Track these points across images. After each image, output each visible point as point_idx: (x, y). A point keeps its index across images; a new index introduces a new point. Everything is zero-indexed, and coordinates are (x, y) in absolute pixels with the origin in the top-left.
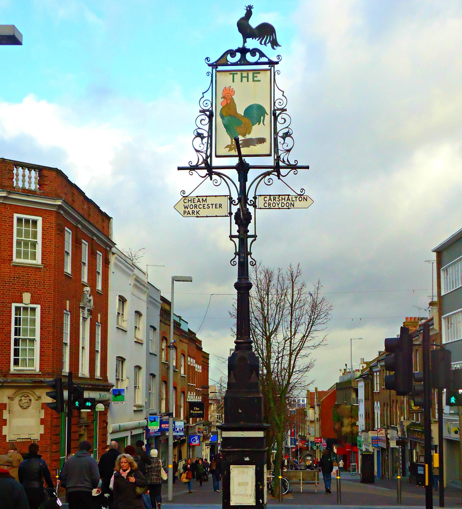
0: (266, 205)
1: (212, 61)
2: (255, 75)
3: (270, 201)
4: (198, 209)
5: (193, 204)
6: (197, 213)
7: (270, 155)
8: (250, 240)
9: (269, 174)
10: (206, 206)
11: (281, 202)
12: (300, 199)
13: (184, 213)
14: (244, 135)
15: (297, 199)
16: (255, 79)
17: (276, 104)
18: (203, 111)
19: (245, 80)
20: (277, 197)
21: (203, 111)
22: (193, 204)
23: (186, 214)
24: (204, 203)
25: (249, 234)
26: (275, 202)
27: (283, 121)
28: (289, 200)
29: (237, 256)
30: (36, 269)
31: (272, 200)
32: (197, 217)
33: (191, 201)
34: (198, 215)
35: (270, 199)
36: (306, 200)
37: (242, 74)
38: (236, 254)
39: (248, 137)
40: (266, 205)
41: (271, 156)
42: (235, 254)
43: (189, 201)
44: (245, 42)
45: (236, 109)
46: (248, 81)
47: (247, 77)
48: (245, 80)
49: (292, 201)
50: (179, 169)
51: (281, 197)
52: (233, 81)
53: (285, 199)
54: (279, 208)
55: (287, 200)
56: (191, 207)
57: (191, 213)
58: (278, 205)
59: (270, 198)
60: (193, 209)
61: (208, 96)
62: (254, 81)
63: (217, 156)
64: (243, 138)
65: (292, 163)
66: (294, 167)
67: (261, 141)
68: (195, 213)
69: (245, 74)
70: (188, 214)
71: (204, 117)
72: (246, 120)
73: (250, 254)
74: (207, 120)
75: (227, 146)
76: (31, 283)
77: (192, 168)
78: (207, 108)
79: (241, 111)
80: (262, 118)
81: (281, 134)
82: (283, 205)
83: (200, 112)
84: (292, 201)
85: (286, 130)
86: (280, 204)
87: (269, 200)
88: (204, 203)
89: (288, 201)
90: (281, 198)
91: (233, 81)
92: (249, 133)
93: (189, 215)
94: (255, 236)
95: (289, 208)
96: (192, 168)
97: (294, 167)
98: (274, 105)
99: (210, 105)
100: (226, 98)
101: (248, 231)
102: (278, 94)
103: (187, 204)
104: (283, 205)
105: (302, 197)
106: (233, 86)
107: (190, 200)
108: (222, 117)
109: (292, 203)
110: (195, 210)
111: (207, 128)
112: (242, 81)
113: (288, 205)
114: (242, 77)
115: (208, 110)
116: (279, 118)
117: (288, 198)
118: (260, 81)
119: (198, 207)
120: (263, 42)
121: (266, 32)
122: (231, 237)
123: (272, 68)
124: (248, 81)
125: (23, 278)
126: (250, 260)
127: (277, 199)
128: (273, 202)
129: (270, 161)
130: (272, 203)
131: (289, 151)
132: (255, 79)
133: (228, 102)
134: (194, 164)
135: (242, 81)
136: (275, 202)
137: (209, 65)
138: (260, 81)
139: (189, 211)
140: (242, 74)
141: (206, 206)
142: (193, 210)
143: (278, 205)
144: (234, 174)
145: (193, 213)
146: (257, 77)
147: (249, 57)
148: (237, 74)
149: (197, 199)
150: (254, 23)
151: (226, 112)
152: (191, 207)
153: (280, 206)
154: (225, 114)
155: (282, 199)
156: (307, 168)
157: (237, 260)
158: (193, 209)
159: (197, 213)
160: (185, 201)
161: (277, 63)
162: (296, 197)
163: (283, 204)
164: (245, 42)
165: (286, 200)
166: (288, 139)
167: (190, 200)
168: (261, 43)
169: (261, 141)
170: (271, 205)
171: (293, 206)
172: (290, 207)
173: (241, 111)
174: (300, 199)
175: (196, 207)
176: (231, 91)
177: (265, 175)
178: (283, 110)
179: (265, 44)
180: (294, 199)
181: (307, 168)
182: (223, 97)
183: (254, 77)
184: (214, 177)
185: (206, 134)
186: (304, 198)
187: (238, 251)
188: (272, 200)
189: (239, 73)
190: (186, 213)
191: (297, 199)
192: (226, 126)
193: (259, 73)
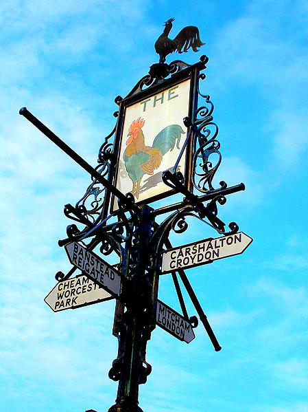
0: (173, 264)
3: (180, 257)
4: (76, 295)
5: (70, 289)
6: (74, 301)
10: (87, 288)
11: (197, 253)
12: (230, 241)
13: (56, 306)
15: (225, 241)
20: (191, 247)
22: (70, 289)
23: (58, 308)
24: (85, 284)
26: (188, 256)
32: (73, 308)
34: (74, 305)
35: (181, 254)
40: (173, 264)
44: (162, 60)
47: (162, 99)
49: (216, 247)
51: (198, 245)
53: (203, 248)
54: (195, 265)
55: (208, 248)
57: (65, 305)
58: (193, 259)
61: (112, 140)
68: (71, 303)
82: (200, 257)
84: (216, 247)
87: (179, 255)
88: (85, 284)
89: (210, 250)
90: (197, 249)
93: (62, 308)
95: (211, 261)
102: (201, 102)
105: (233, 236)
106: (144, 116)
107: (67, 284)
108: (126, 159)
109: (216, 250)
110: (71, 298)
113: (208, 256)
114: (155, 100)
117: (210, 244)
119: (75, 293)
120: (182, 50)
121: (190, 36)
127: (192, 251)
128: (185, 257)
130: (183, 258)
136: (188, 256)
141: (87, 288)
143: (193, 259)
145: (68, 303)
149: (76, 280)
150: (172, 36)
153: (196, 261)
155: (200, 248)
156: (241, 187)
159: (74, 301)
162: (222, 240)
163: (200, 257)
164: (162, 60)
165: (206, 248)
168: (180, 52)
170: (182, 263)
171: (218, 255)
172: (211, 259)
173: (149, 142)
174: (230, 241)
179: (185, 51)
180: (219, 243)
181: (241, 187)
188: (184, 255)
190: (59, 307)
191: (225, 241)
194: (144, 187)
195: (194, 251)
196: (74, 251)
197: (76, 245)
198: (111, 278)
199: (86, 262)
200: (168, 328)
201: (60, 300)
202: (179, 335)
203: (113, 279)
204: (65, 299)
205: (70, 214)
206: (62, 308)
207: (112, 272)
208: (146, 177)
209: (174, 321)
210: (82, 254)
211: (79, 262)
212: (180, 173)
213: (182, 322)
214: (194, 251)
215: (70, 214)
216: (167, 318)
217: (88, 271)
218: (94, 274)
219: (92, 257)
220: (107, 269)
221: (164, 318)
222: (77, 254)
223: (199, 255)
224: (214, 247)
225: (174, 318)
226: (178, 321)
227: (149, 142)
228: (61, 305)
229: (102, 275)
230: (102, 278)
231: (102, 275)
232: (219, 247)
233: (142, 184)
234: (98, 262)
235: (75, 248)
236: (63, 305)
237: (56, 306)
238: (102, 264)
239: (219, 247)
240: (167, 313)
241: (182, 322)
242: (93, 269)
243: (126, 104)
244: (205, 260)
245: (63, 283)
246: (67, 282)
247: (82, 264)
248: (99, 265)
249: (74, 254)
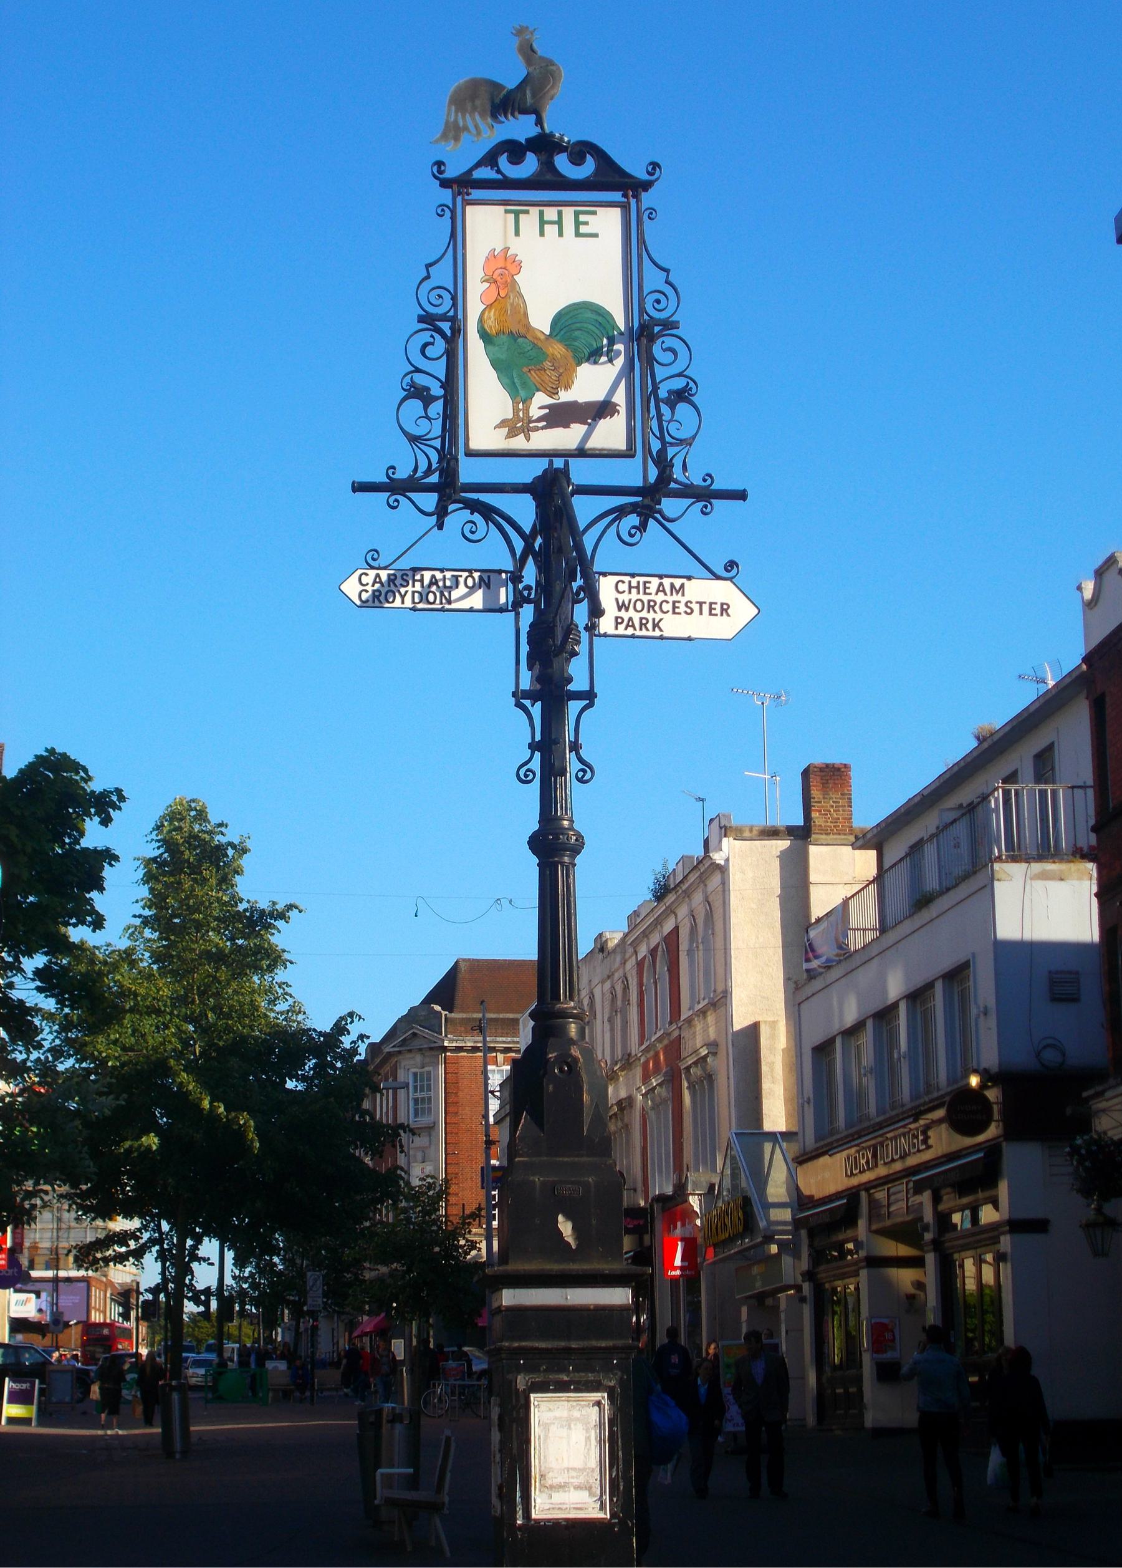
1: (451, 173)
2: (582, 218)
7: (629, 454)
8: (574, 707)
9: (620, 512)
14: (553, 393)
16: (583, 229)
17: (649, 307)
18: (428, 320)
19: (551, 230)
21: (428, 320)
25: (571, 687)
27: (669, 357)
29: (537, 755)
37: (541, 214)
38: (534, 747)
39: (564, 396)
41: (633, 456)
42: (530, 746)
45: (526, 314)
46: (561, 234)
47: (559, 223)
48: (551, 230)
50: (360, 487)
52: (517, 233)
62: (578, 234)
63: (470, 454)
64: (550, 401)
65: (697, 481)
66: (704, 495)
67: (604, 409)
69: (551, 213)
71: (425, 337)
72: (557, 349)
73: (575, 747)
74: (440, 345)
75: (503, 423)
77: (397, 487)
78: (440, 311)
79: (541, 320)
81: (663, 393)
83: (421, 319)
85: (679, 384)
91: (517, 233)
92: (568, 387)
94: (589, 696)
96: (397, 487)
97: (704, 495)
98: (642, 310)
99: (448, 303)
100: (495, 281)
101: (570, 680)
102: (653, 279)
106: (517, 247)
108: (484, 335)
111: (439, 369)
112: (542, 234)
114: (543, 223)
115: (444, 318)
116: (657, 350)
118: (596, 235)
122: (519, 696)
123: (633, 201)
124: (561, 234)
126: (573, 766)
129: (631, 473)
131: (687, 442)
132: (583, 229)
133: (502, 294)
134: (402, 473)
135: (542, 234)
137: (445, 184)
138: (596, 235)
140: (541, 214)
144: (523, 510)
146: (586, 223)
147: (562, 162)
148: (527, 212)
156: (742, 495)
157: (536, 764)
161: (646, 186)
166: (682, 408)
169: (604, 409)
173: (541, 320)
177: (620, 512)
178: (669, 325)
181: (742, 495)
182: (490, 279)
183: (578, 224)
184: (458, 517)
185: (437, 390)
187: (538, 738)
189: (534, 211)
192: (495, 364)
193: (595, 213)
194: (539, 420)
208: (541, 400)
233: (535, 412)
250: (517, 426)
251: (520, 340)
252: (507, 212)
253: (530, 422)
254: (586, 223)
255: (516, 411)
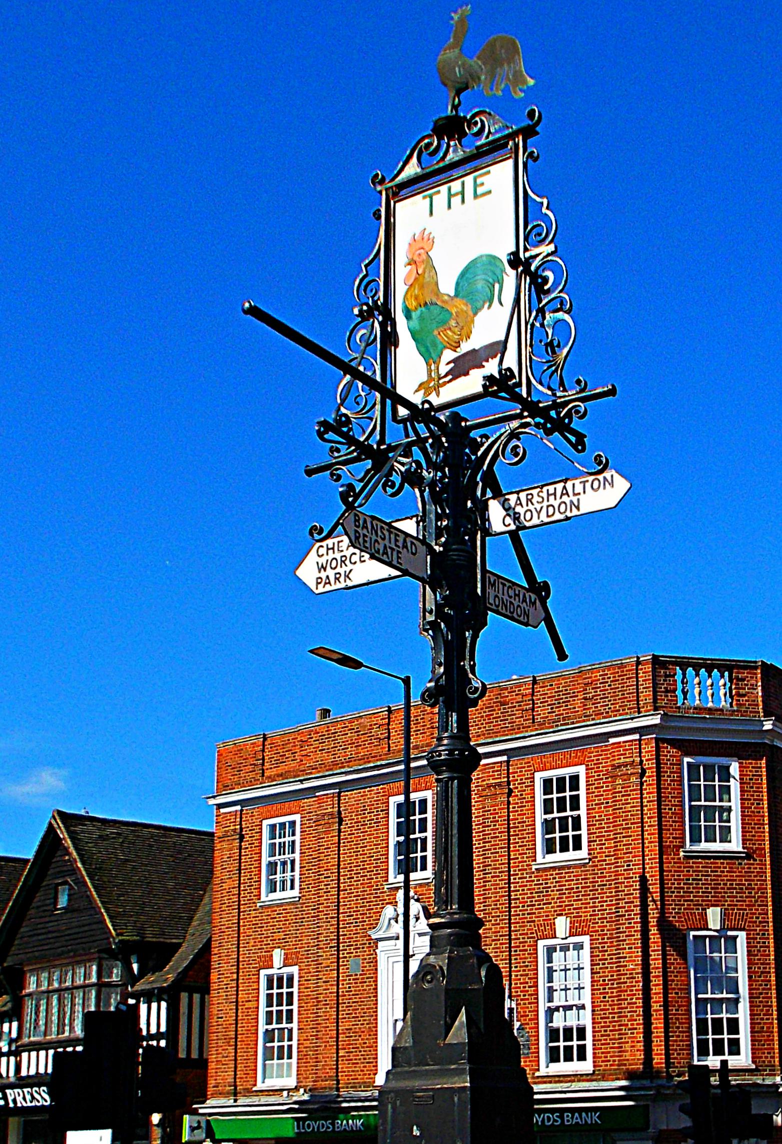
4: (350, 566)
5: (338, 556)
6: (347, 576)
11: (545, 504)
13: (318, 583)
14: (455, 347)
15: (588, 485)
16: (480, 191)
19: (456, 200)
20: (535, 492)
22: (338, 556)
28: (567, 494)
30: (729, 857)
31: (524, 502)
33: (333, 549)
36: (612, 484)
43: (328, 549)
46: (463, 201)
51: (545, 489)
53: (555, 494)
55: (562, 494)
56: (334, 564)
59: (519, 498)
60: (338, 570)
62: (476, 196)
68: (342, 579)
69: (456, 186)
70: (326, 583)
72: (460, 305)
76: (723, 888)
80: (497, 286)
82: (551, 510)
84: (575, 494)
86: (544, 510)
89: (565, 498)
90: (544, 495)
103: (322, 561)
104: (550, 513)
105: (601, 477)
106: (433, 226)
107: (330, 546)
109: (575, 499)
117: (564, 487)
119: (347, 562)
124: (463, 201)
125: (707, 880)
127: (536, 499)
128: (525, 508)
132: (480, 191)
133: (420, 272)
136: (530, 507)
138: (490, 192)
139: (328, 577)
142: (337, 571)
143: (539, 513)
145: (337, 579)
146: (482, 184)
148: (439, 192)
151: (416, 298)
152: (334, 565)
154: (412, 304)
158: (338, 570)
160: (323, 551)
163: (551, 509)
167: (330, 546)
171: (578, 508)
172: (569, 514)
175: (344, 562)
176: (426, 239)
186: (605, 478)
188: (524, 502)
191: (588, 485)
192: (414, 335)
193: (489, 172)
195: (540, 500)
196: (356, 526)
197: (356, 515)
198: (412, 553)
199: (374, 537)
200: (504, 611)
201: (323, 575)
202: (521, 618)
203: (414, 554)
204: (331, 573)
205: (326, 436)
206: (328, 588)
207: (412, 543)
208: (449, 355)
209: (511, 597)
210: (367, 528)
211: (365, 541)
212: (509, 369)
213: (524, 596)
214: (540, 500)
215: (326, 436)
216: (500, 596)
217: (378, 552)
218: (387, 554)
219: (382, 528)
220: (405, 541)
221: (496, 596)
222: (359, 530)
223: (548, 506)
224: (571, 493)
225: (511, 593)
226: (519, 595)
227: (447, 286)
228: (326, 583)
229: (399, 552)
230: (399, 558)
231: (399, 552)
232: (579, 494)
234: (390, 533)
235: (356, 521)
236: (329, 583)
237: (318, 583)
238: (397, 535)
239: (579, 494)
240: (501, 586)
241: (524, 596)
242: (385, 546)
243: (395, 194)
244: (558, 516)
245: (324, 544)
246: (330, 542)
247: (368, 545)
248: (392, 536)
249: (356, 531)
250: (432, 384)
251: (432, 308)
252: (424, 197)
253: (440, 379)
254: (482, 184)
255: (429, 371)
